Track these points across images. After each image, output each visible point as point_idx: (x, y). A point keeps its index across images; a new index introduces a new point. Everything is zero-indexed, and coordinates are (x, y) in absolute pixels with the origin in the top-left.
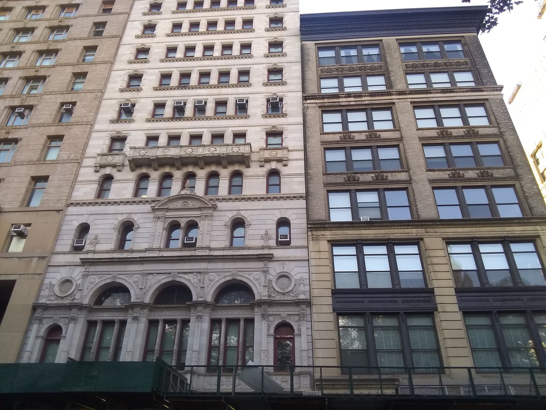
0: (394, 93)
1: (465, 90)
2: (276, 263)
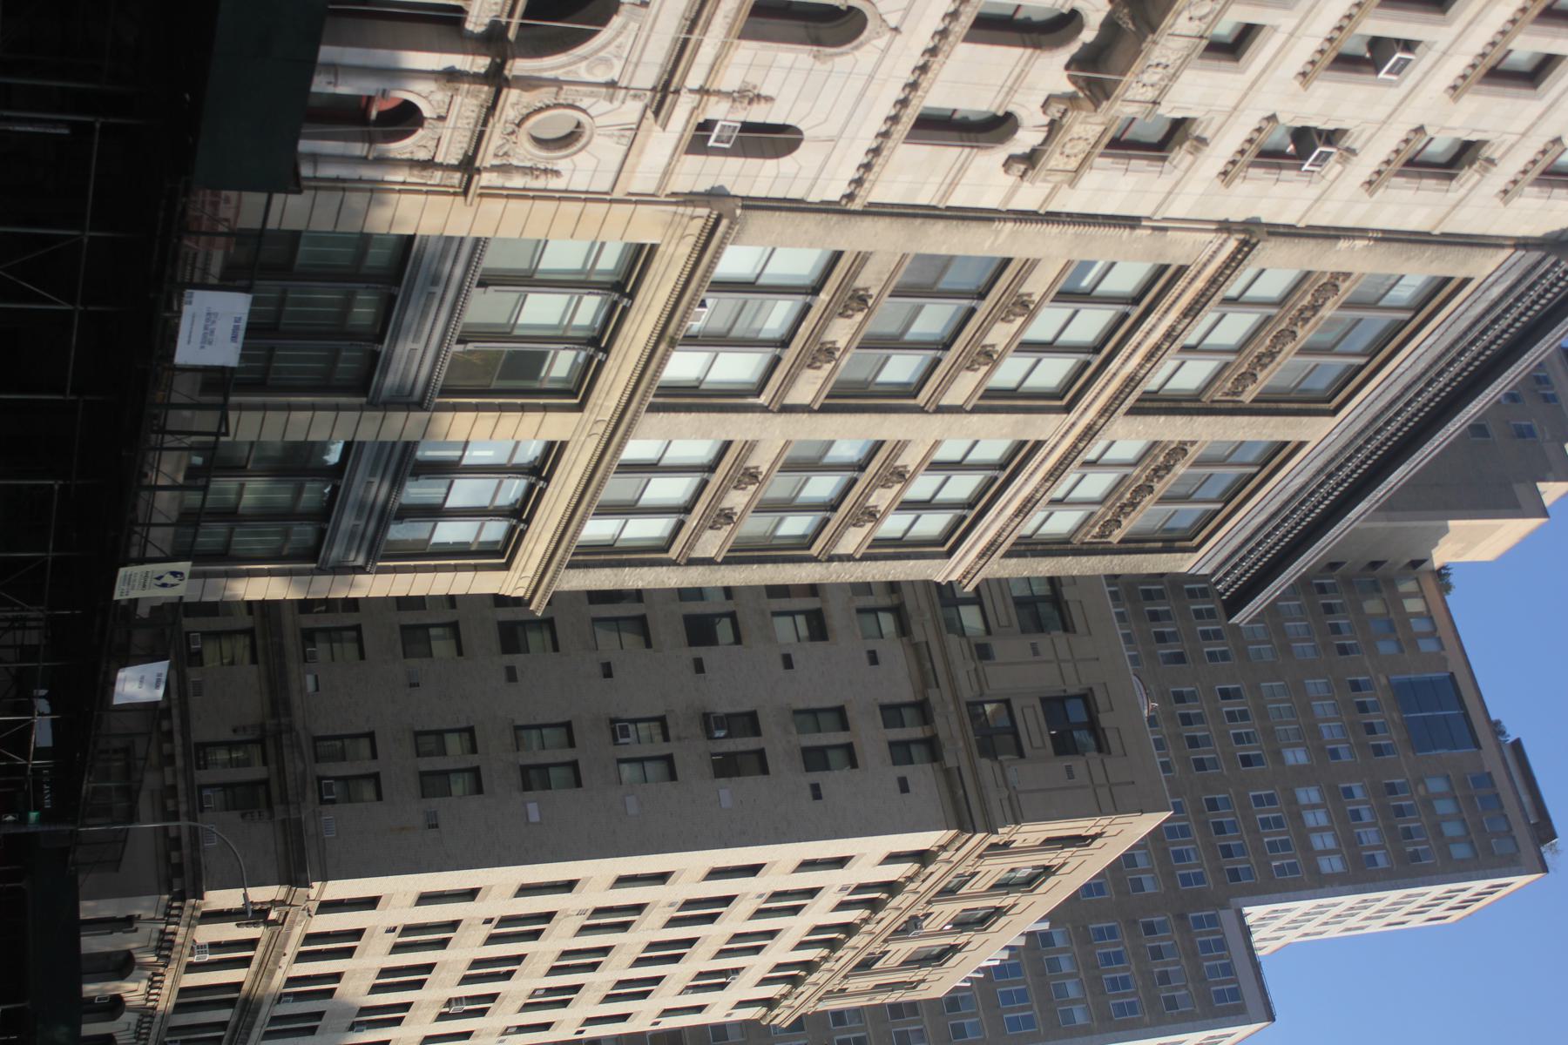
0: (1102, 421)
1: (1005, 534)
2: (635, 117)
